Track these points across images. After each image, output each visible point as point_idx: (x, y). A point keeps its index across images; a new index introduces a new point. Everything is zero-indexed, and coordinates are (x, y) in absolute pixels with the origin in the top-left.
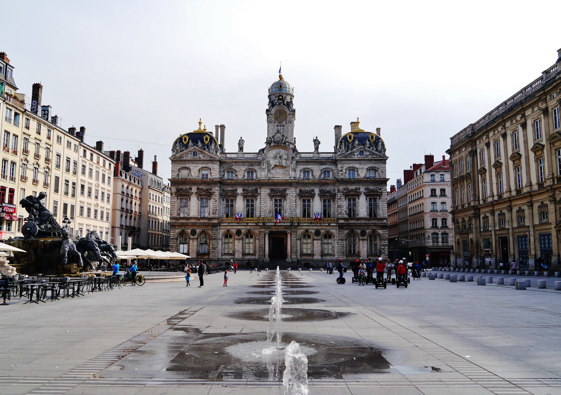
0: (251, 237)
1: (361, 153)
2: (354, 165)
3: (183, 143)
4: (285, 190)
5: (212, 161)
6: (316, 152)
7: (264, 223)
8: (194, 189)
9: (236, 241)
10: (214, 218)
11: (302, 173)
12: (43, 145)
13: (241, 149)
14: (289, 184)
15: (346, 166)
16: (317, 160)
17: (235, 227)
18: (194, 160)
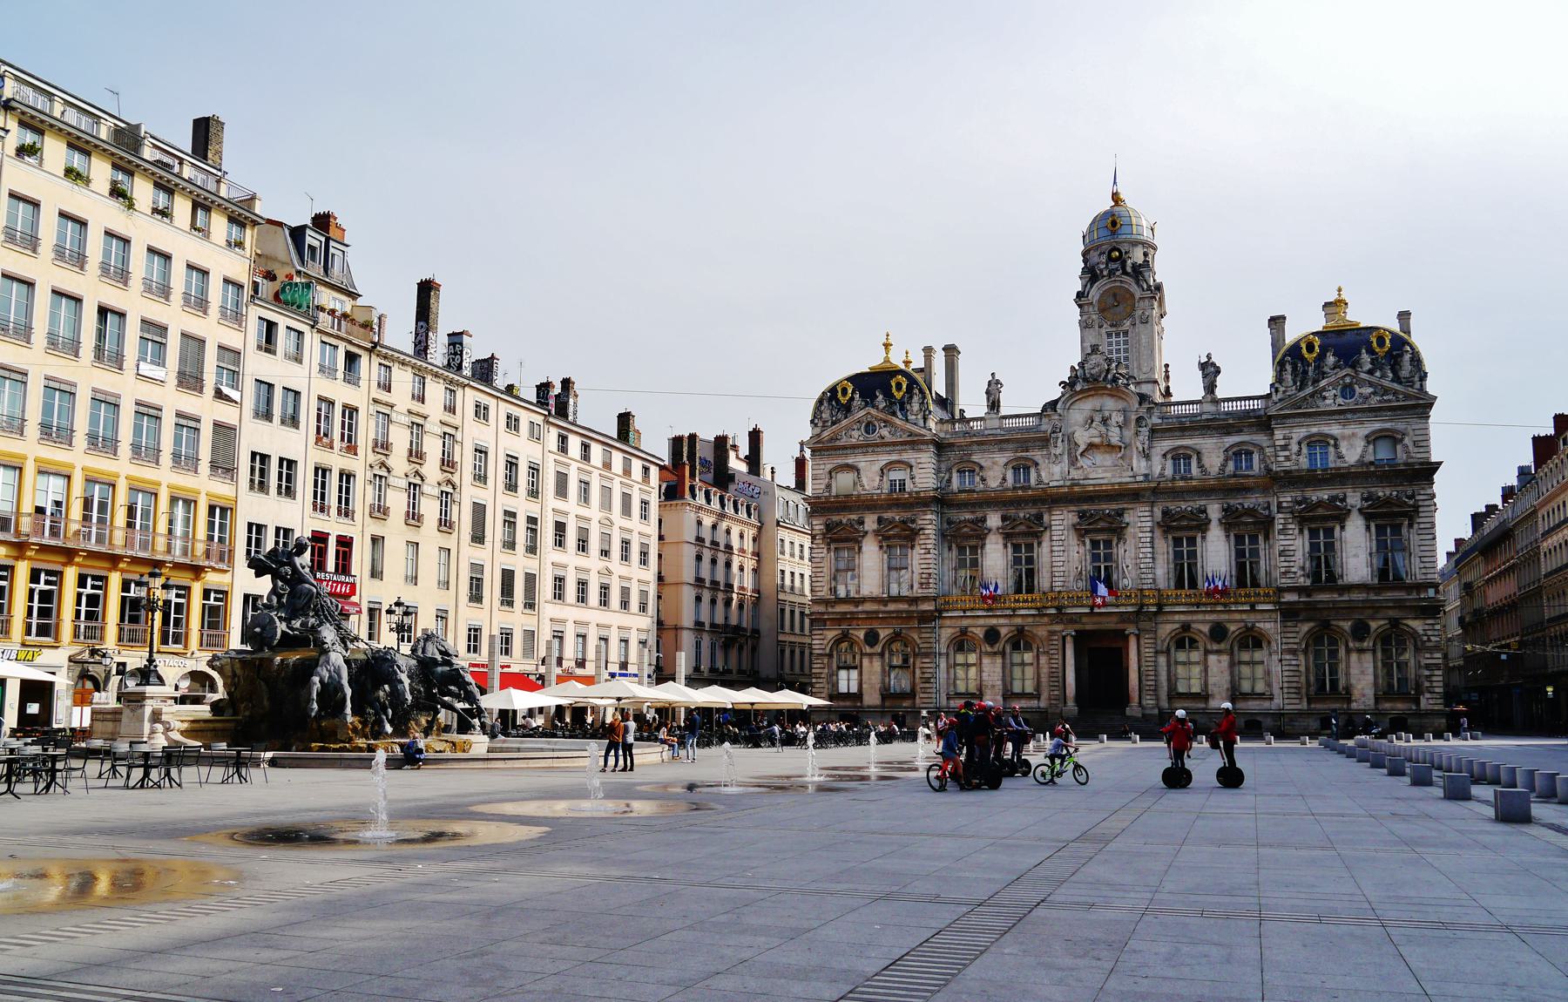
0: (1028, 648)
1: (1347, 391)
2: (1326, 430)
3: (838, 401)
4: (1120, 513)
5: (915, 443)
6: (1209, 398)
7: (1059, 608)
8: (870, 522)
9: (986, 661)
10: (925, 599)
11: (1169, 463)
12: (433, 426)
13: (994, 405)
14: (1132, 495)
15: (1300, 433)
16: (1216, 420)
17: (981, 622)
18: (868, 446)
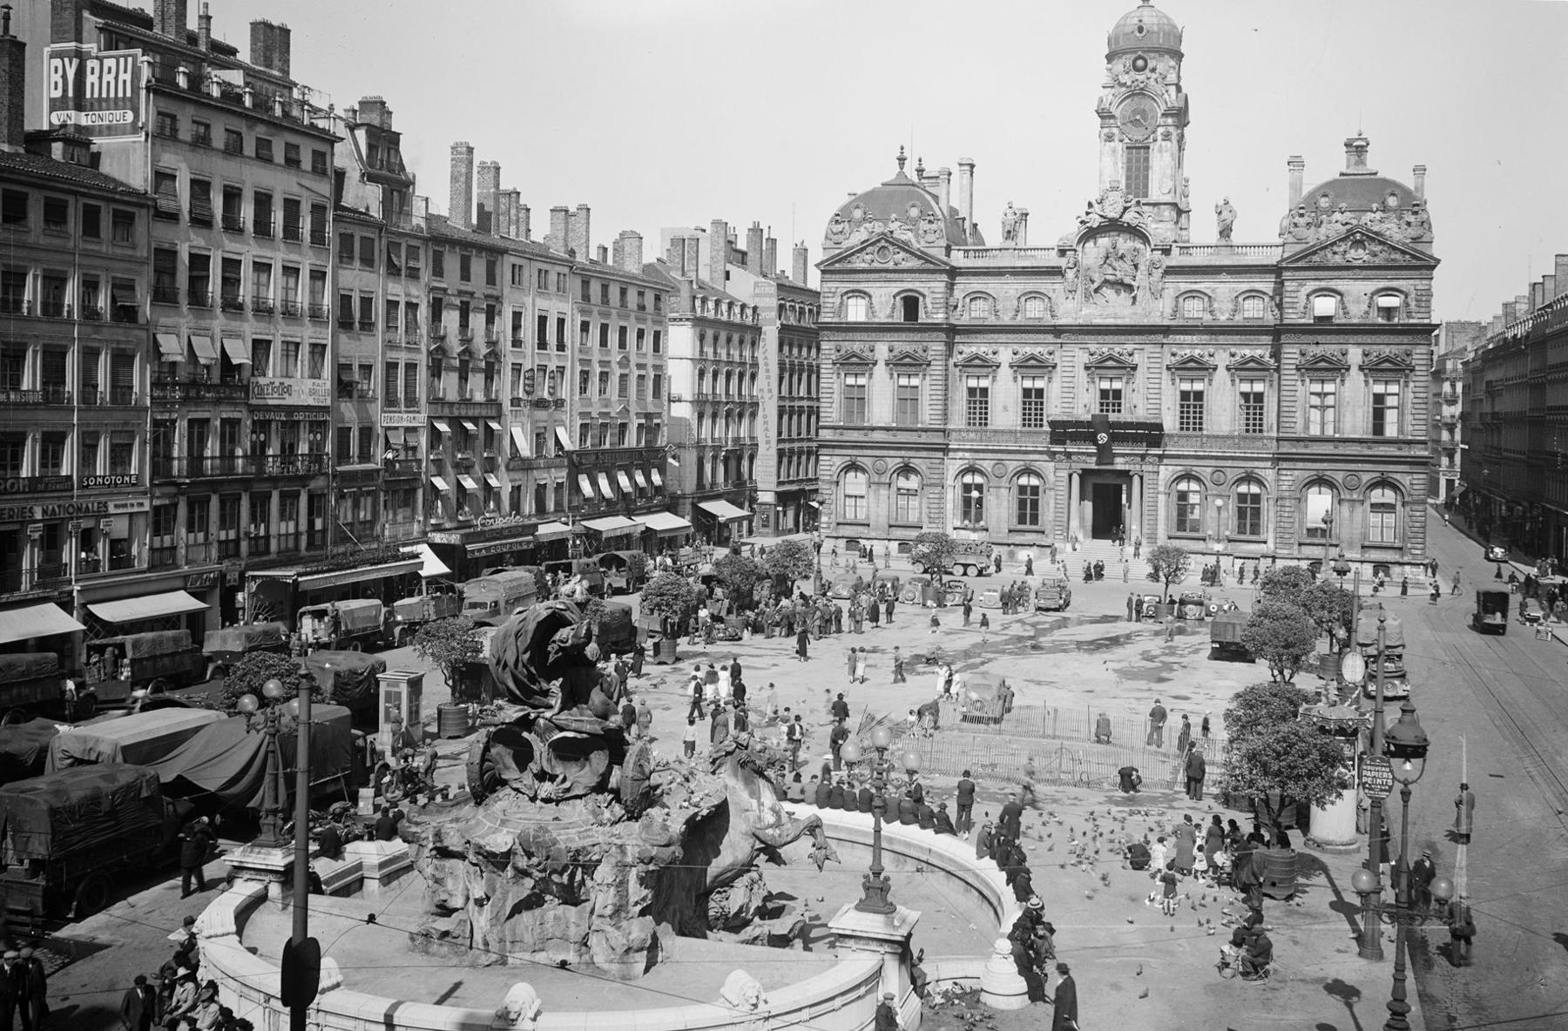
6: (1223, 242)
